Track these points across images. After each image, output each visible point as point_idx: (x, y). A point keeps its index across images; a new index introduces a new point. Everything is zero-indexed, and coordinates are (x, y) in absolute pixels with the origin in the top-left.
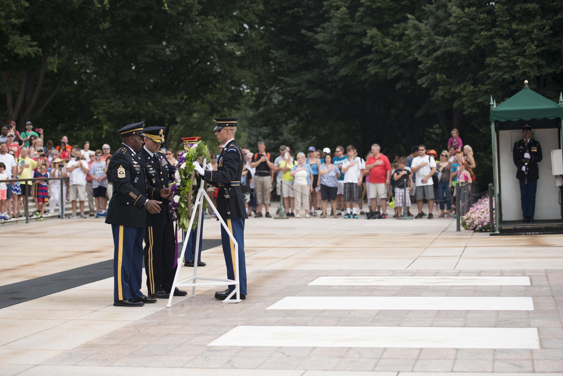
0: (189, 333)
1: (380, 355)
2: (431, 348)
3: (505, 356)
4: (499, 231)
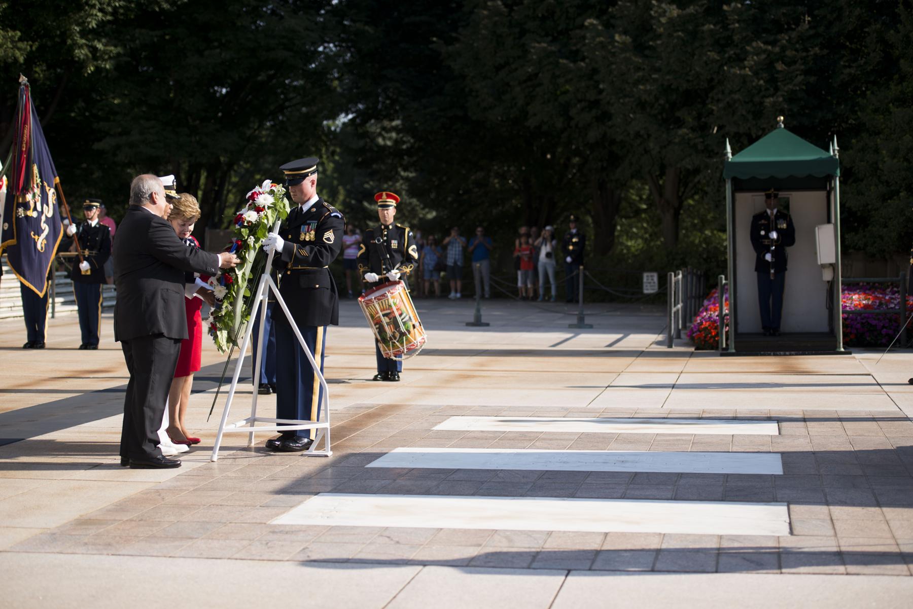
0: (242, 504)
2: (622, 533)
4: (736, 348)
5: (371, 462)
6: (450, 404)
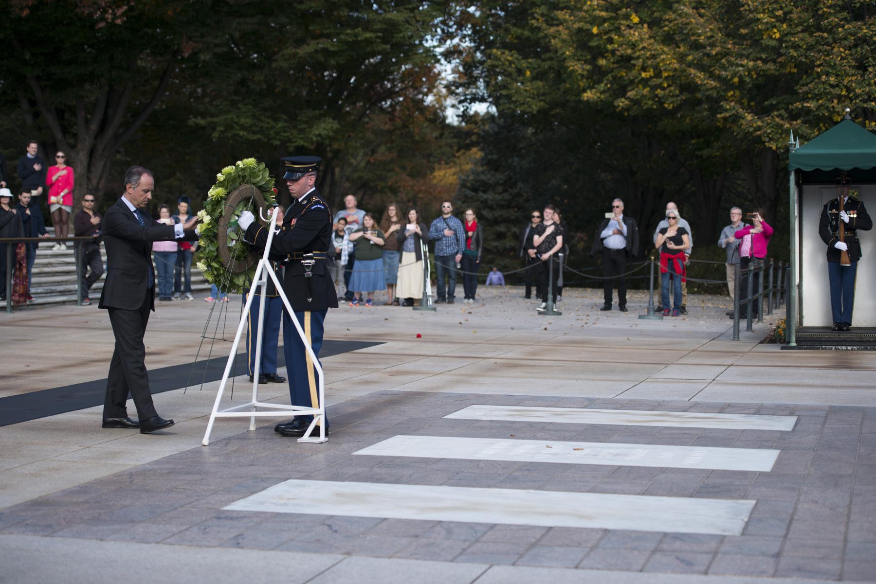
1: (479, 534)
3: (678, 545)
4: (797, 341)
5: (361, 449)
6: (477, 393)
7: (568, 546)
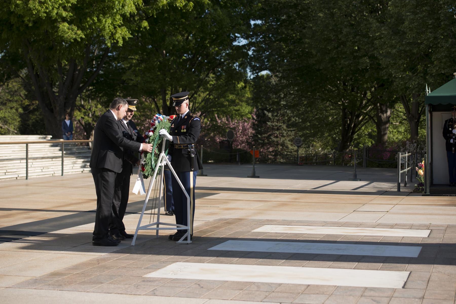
3: (372, 293)
5: (211, 247)
7: (318, 294)
